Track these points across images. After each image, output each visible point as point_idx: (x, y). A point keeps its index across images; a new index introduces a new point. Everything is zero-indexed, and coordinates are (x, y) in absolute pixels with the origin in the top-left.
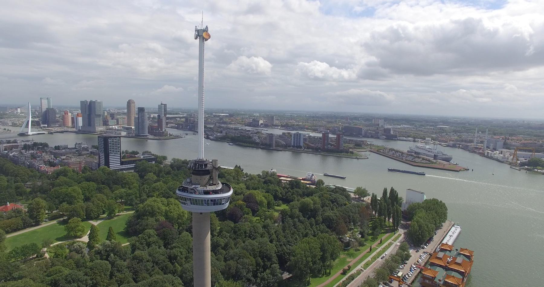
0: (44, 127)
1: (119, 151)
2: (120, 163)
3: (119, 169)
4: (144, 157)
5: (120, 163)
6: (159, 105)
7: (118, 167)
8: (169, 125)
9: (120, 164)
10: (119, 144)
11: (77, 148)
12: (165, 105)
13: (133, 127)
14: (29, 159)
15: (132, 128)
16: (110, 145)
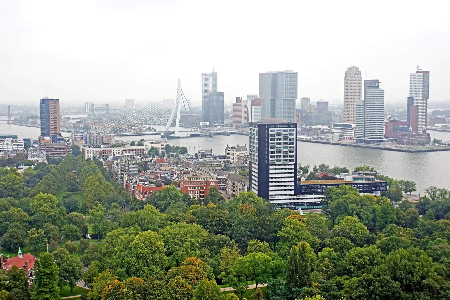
0: (205, 126)
1: (291, 160)
2: (293, 188)
3: (291, 204)
4: (354, 179)
5: (293, 188)
6: (411, 75)
7: (289, 197)
8: (436, 125)
9: (293, 192)
10: (293, 143)
11: (228, 156)
12: (426, 74)
13: (354, 125)
14: (135, 171)
15: (351, 125)
16: (271, 143)
